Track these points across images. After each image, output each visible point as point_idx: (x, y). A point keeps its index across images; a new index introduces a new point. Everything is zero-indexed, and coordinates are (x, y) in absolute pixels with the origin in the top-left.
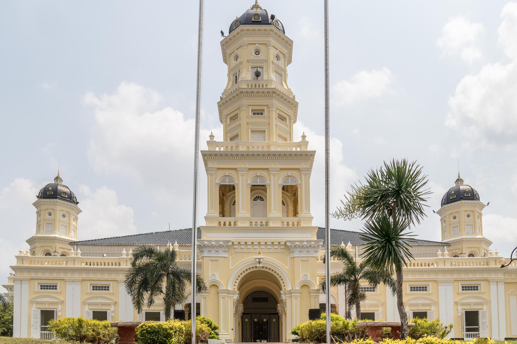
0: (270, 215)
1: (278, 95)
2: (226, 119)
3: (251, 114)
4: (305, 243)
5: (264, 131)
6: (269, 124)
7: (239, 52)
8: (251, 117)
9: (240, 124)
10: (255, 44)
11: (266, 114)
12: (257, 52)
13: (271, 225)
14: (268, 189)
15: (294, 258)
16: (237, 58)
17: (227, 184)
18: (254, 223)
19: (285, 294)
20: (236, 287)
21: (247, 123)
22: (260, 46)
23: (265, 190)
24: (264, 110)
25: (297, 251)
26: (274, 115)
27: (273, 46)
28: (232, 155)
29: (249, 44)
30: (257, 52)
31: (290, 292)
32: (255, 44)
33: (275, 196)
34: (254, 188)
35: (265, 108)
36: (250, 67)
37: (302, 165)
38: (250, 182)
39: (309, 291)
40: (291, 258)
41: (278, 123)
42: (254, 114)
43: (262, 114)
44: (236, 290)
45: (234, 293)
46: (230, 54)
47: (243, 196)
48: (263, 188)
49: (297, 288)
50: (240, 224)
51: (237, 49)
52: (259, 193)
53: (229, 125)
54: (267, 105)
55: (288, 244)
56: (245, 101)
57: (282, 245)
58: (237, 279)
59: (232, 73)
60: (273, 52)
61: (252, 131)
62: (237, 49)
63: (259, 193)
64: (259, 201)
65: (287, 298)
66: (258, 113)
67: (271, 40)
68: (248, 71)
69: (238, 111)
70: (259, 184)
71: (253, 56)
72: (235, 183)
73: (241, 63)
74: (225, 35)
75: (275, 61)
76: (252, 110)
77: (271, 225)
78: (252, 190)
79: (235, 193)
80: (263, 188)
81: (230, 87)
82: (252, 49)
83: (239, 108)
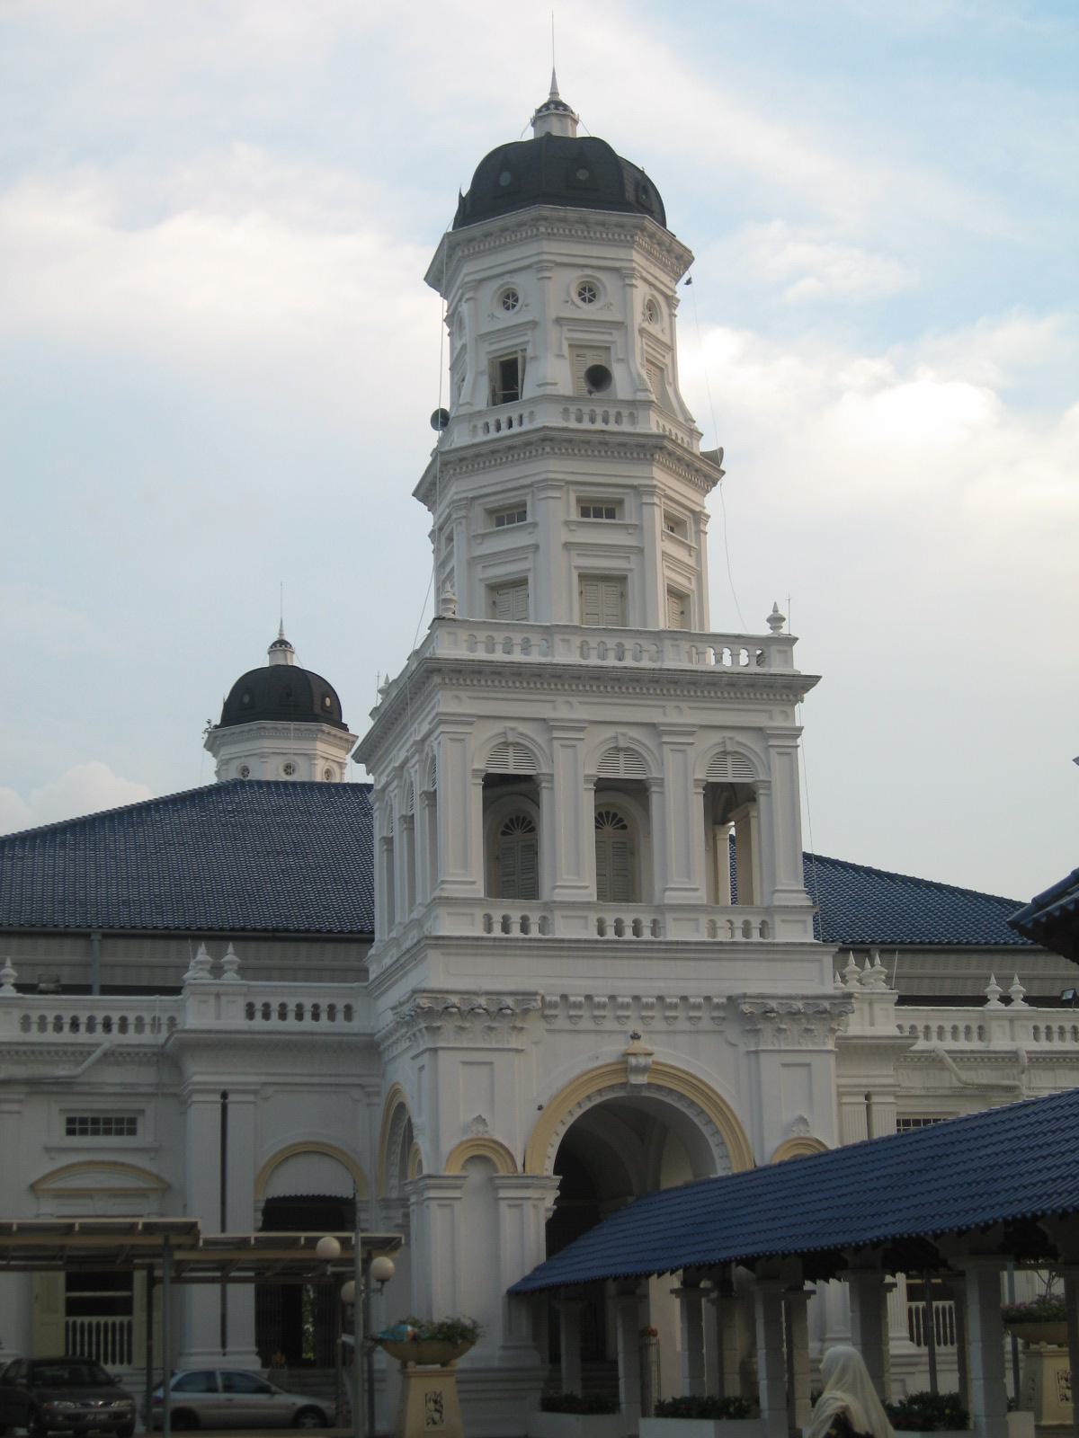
6: (641, 551)
7: (522, 283)
11: (629, 515)
12: (588, 292)
13: (676, 931)
23: (646, 806)
24: (620, 502)
27: (645, 280)
34: (603, 786)
36: (565, 345)
42: (585, 512)
43: (611, 514)
48: (638, 791)
56: (556, 467)
63: (622, 807)
66: (599, 509)
67: (636, 256)
68: (560, 356)
76: (579, 500)
80: (638, 791)
82: (572, 279)
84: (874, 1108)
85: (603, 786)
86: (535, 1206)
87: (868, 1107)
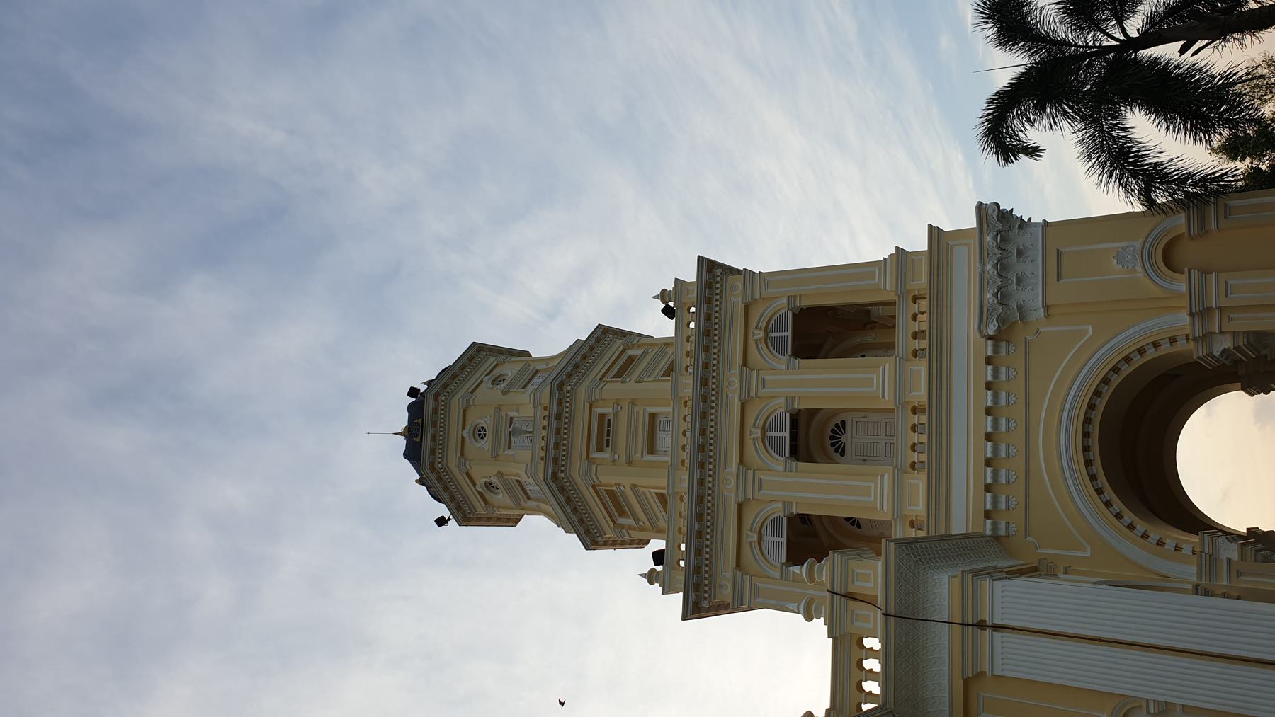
0: (887, 400)
1: (569, 375)
2: (622, 526)
3: (606, 455)
4: (989, 267)
5: (653, 416)
6: (633, 402)
7: (481, 481)
8: (614, 451)
10: (463, 438)
11: (608, 411)
12: (480, 433)
13: (920, 394)
14: (804, 405)
15: (1046, 307)
16: (490, 486)
17: (784, 540)
18: (915, 457)
19: (1207, 337)
21: (630, 464)
23: (813, 412)
24: (602, 416)
26: (614, 388)
28: (700, 517)
29: (462, 454)
30: (480, 433)
31: (1201, 314)
32: (463, 438)
33: (828, 383)
34: (799, 450)
35: (598, 410)
37: (736, 295)
38: (779, 462)
40: (1047, 315)
41: (634, 377)
46: (486, 501)
47: (824, 489)
49: (1183, 288)
51: (475, 485)
52: (814, 437)
53: (636, 519)
54: (591, 406)
55: (991, 329)
56: (576, 471)
57: (996, 349)
59: (523, 503)
60: (488, 394)
61: (651, 451)
62: (475, 485)
63: (814, 437)
64: (847, 438)
65: (1229, 327)
66: (604, 433)
70: (787, 434)
71: (485, 444)
72: (777, 510)
73: (500, 474)
74: (447, 514)
75: (502, 386)
76: (600, 449)
78: (810, 459)
79: (820, 516)
80: (801, 422)
81: (549, 509)
83: (594, 487)
84: (997, 621)
85: (799, 450)
86: (1239, 574)
87: (996, 627)
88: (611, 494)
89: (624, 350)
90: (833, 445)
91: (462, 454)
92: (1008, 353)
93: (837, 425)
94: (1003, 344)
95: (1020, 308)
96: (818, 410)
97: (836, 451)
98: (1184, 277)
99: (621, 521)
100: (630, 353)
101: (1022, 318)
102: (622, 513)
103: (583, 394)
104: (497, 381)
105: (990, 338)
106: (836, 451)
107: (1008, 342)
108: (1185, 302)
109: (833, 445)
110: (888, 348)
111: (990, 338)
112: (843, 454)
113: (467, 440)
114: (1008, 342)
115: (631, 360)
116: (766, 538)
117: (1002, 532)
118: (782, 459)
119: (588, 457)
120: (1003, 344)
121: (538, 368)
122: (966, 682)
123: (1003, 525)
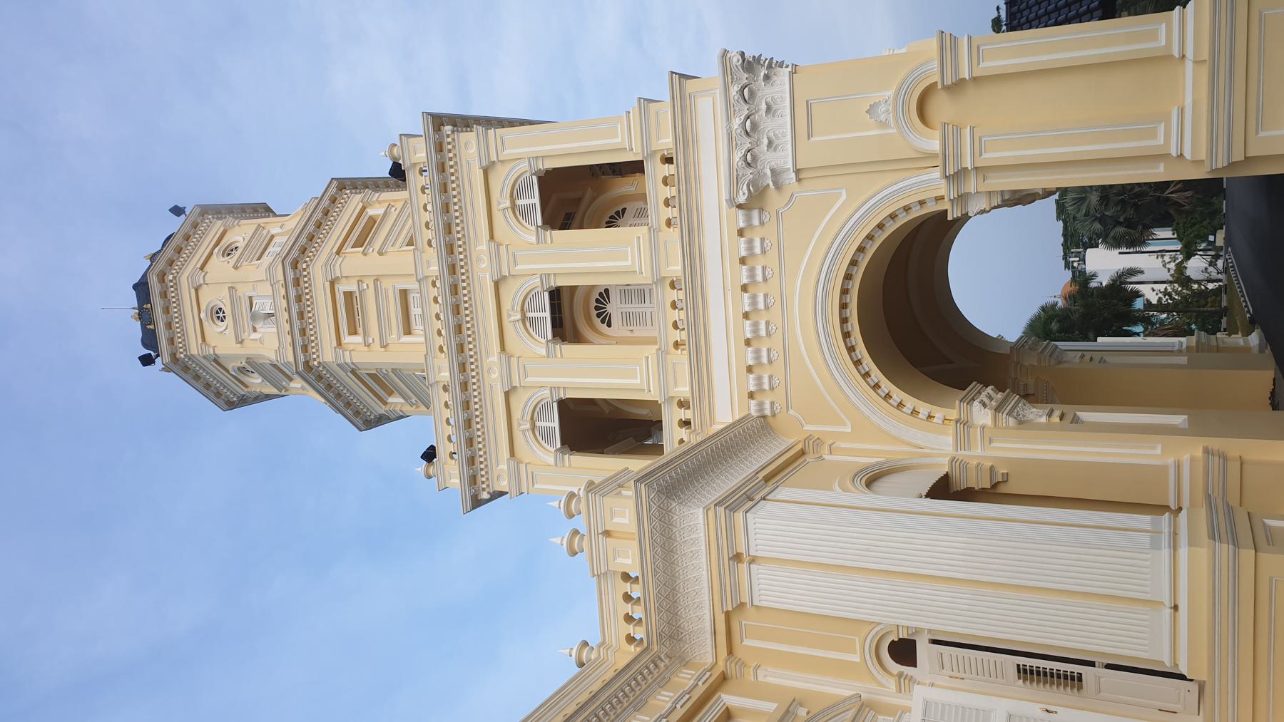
0: (645, 278)
3: (358, 339)
9: (394, 371)
10: (200, 320)
11: (352, 287)
12: (218, 314)
13: (675, 268)
14: (561, 282)
15: (797, 172)
20: (939, 413)
22: (203, 307)
25: (769, 160)
26: (355, 264)
29: (204, 339)
30: (218, 314)
31: (957, 177)
32: (200, 320)
33: (585, 256)
36: (254, 336)
39: (947, 88)
40: (799, 180)
44: (953, 414)
45: (964, 424)
50: (683, 390)
54: (332, 283)
57: (748, 219)
58: (900, 405)
69: (362, 372)
70: (547, 314)
76: (353, 332)
77: (675, 268)
78: (577, 338)
82: (213, 329)
88: (371, 376)
89: (364, 208)
90: (598, 315)
91: (204, 339)
92: (762, 223)
93: (601, 294)
94: (755, 213)
95: (772, 171)
96: (576, 287)
97: (603, 322)
98: (937, 134)
99: (391, 400)
100: (371, 212)
101: (775, 183)
102: (390, 393)
103: (317, 272)
104: (228, 252)
105: (740, 207)
106: (603, 322)
107: (761, 210)
108: (939, 162)
109: (598, 315)
110: (642, 213)
111: (740, 207)
112: (609, 325)
113: (206, 324)
114: (761, 210)
115: (372, 220)
116: (538, 424)
117: (768, 412)
118: (543, 341)
119: (339, 343)
120: (755, 213)
121: (273, 232)
122: (728, 615)
123: (767, 406)
